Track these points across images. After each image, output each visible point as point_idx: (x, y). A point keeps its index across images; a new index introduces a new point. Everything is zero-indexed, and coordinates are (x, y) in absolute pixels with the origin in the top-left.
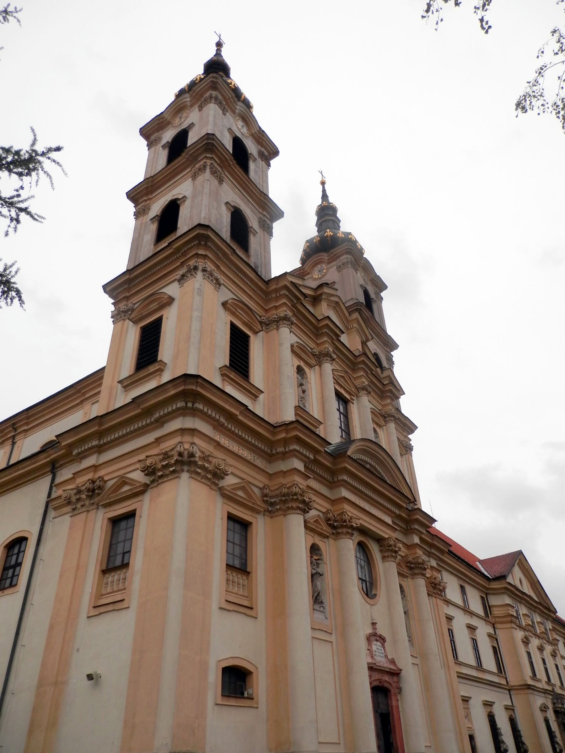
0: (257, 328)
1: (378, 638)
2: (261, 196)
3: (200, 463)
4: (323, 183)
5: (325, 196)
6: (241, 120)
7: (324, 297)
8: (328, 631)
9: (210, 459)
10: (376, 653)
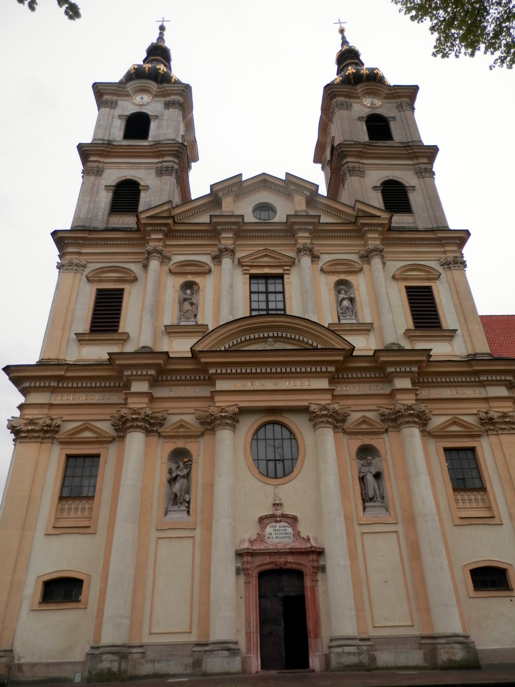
0: (130, 277)
1: (279, 519)
2: (152, 149)
3: (25, 428)
4: (342, 31)
6: (136, 95)
7: (220, 194)
8: (186, 528)
9: (35, 421)
10: (270, 536)
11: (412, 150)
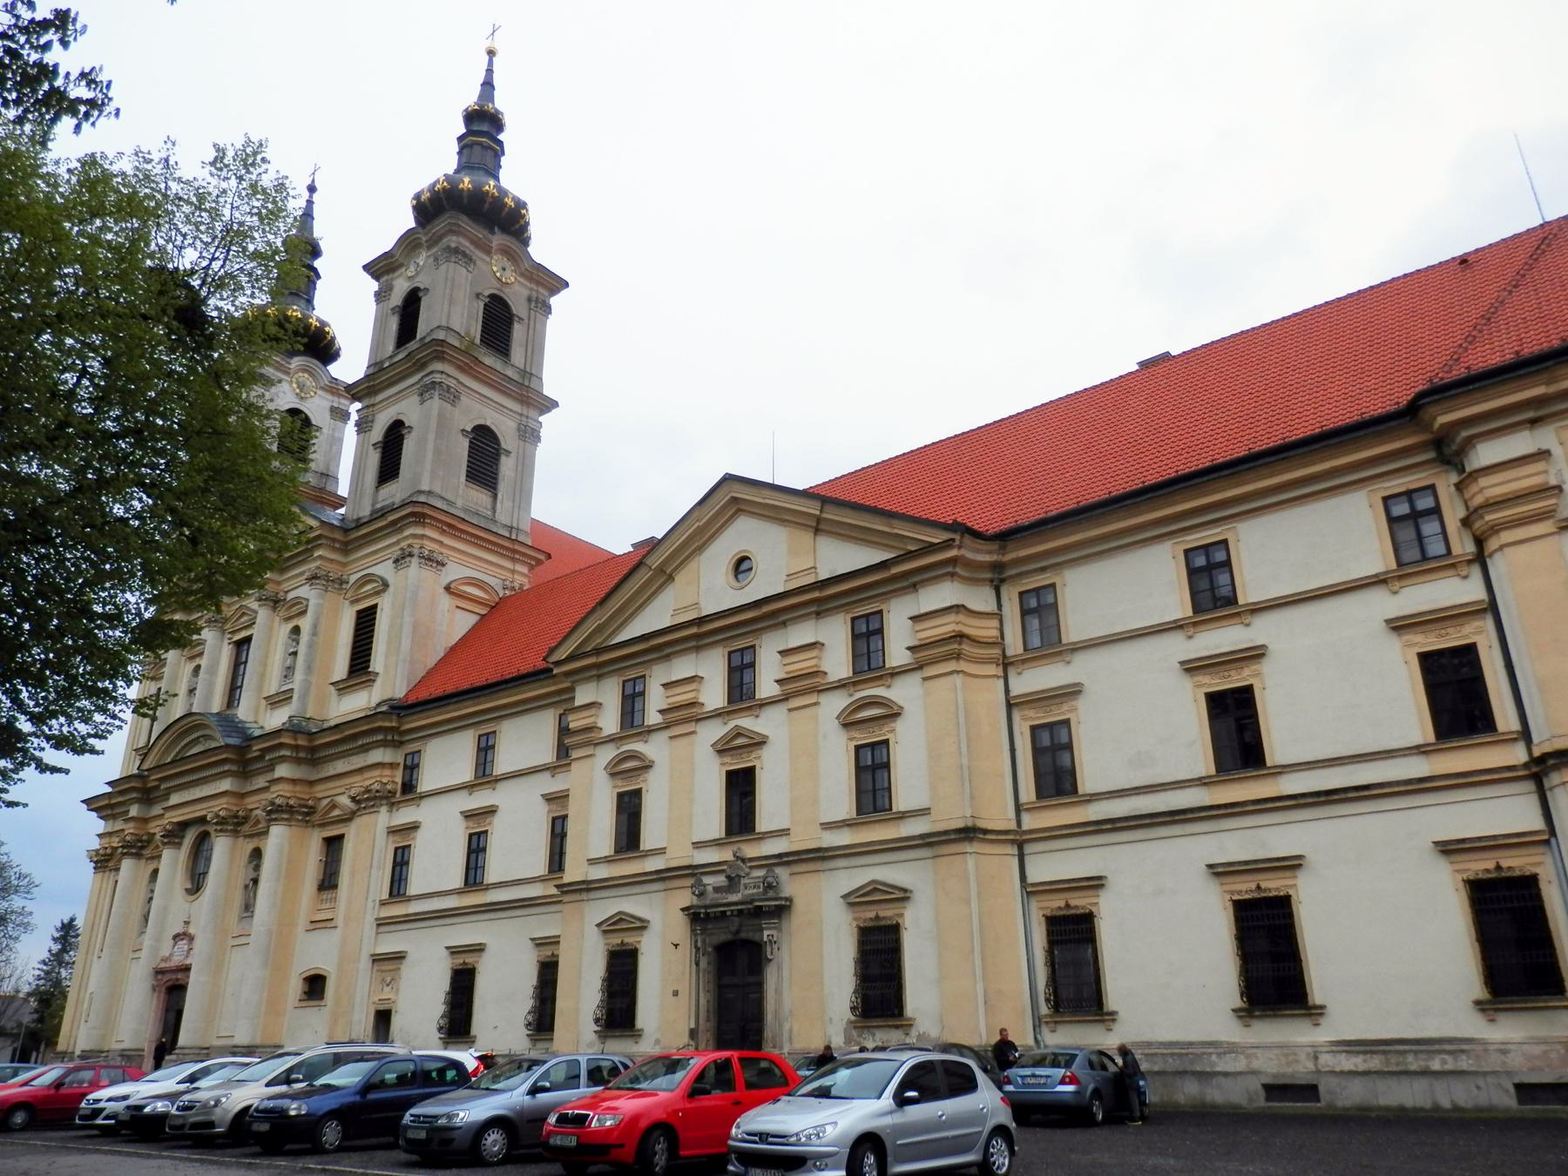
4: (491, 53)
5: (488, 85)
11: (528, 392)
